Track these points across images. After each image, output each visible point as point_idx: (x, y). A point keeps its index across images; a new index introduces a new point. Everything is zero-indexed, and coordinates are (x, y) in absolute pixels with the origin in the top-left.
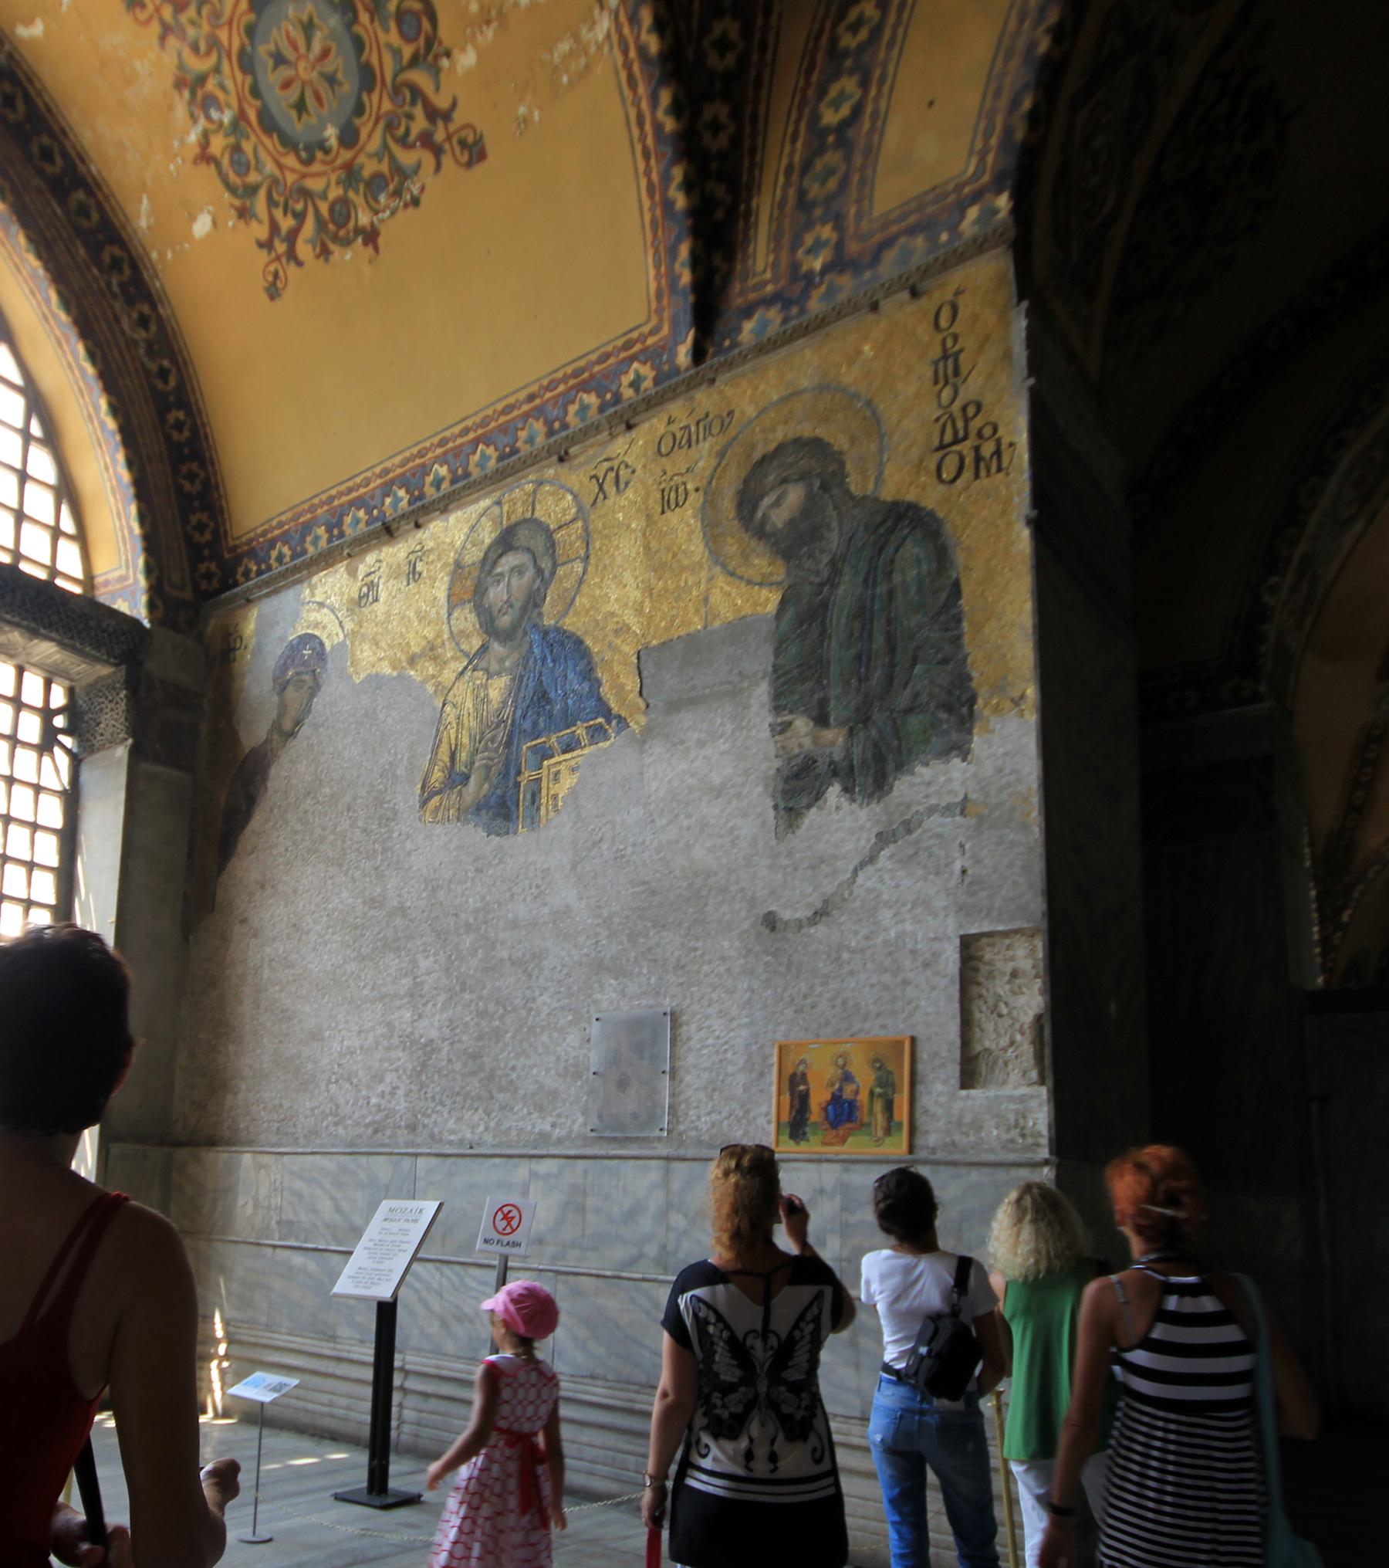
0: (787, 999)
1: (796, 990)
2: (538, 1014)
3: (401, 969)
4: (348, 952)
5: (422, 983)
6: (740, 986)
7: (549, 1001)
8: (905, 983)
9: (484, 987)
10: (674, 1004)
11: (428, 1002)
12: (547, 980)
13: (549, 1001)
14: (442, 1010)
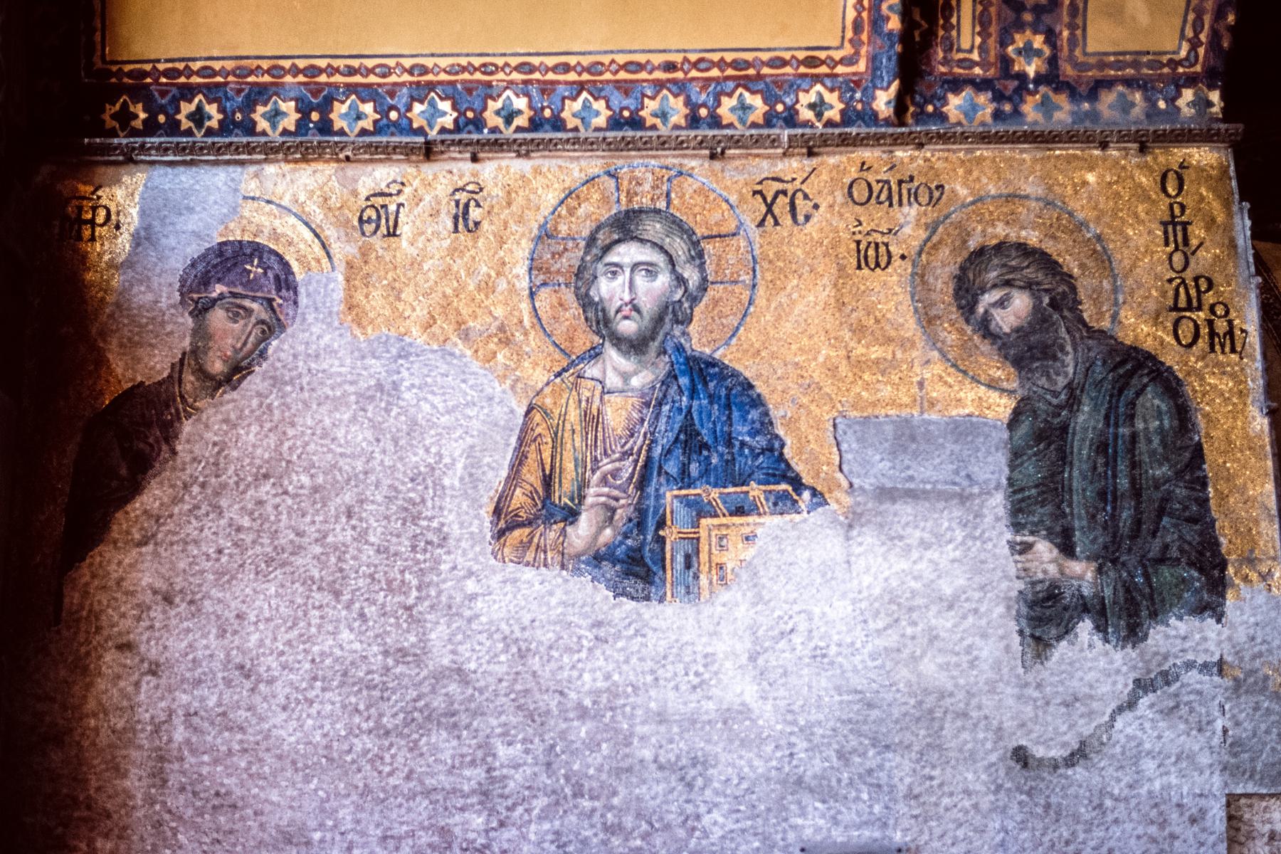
0: (1047, 845)
1: (1056, 834)
2: (706, 834)
3: (462, 756)
4: (357, 720)
5: (505, 777)
6: (991, 825)
7: (721, 820)
9: (615, 793)
10: (908, 839)
11: (515, 805)
12: (717, 793)
13: (721, 820)
14: (539, 818)
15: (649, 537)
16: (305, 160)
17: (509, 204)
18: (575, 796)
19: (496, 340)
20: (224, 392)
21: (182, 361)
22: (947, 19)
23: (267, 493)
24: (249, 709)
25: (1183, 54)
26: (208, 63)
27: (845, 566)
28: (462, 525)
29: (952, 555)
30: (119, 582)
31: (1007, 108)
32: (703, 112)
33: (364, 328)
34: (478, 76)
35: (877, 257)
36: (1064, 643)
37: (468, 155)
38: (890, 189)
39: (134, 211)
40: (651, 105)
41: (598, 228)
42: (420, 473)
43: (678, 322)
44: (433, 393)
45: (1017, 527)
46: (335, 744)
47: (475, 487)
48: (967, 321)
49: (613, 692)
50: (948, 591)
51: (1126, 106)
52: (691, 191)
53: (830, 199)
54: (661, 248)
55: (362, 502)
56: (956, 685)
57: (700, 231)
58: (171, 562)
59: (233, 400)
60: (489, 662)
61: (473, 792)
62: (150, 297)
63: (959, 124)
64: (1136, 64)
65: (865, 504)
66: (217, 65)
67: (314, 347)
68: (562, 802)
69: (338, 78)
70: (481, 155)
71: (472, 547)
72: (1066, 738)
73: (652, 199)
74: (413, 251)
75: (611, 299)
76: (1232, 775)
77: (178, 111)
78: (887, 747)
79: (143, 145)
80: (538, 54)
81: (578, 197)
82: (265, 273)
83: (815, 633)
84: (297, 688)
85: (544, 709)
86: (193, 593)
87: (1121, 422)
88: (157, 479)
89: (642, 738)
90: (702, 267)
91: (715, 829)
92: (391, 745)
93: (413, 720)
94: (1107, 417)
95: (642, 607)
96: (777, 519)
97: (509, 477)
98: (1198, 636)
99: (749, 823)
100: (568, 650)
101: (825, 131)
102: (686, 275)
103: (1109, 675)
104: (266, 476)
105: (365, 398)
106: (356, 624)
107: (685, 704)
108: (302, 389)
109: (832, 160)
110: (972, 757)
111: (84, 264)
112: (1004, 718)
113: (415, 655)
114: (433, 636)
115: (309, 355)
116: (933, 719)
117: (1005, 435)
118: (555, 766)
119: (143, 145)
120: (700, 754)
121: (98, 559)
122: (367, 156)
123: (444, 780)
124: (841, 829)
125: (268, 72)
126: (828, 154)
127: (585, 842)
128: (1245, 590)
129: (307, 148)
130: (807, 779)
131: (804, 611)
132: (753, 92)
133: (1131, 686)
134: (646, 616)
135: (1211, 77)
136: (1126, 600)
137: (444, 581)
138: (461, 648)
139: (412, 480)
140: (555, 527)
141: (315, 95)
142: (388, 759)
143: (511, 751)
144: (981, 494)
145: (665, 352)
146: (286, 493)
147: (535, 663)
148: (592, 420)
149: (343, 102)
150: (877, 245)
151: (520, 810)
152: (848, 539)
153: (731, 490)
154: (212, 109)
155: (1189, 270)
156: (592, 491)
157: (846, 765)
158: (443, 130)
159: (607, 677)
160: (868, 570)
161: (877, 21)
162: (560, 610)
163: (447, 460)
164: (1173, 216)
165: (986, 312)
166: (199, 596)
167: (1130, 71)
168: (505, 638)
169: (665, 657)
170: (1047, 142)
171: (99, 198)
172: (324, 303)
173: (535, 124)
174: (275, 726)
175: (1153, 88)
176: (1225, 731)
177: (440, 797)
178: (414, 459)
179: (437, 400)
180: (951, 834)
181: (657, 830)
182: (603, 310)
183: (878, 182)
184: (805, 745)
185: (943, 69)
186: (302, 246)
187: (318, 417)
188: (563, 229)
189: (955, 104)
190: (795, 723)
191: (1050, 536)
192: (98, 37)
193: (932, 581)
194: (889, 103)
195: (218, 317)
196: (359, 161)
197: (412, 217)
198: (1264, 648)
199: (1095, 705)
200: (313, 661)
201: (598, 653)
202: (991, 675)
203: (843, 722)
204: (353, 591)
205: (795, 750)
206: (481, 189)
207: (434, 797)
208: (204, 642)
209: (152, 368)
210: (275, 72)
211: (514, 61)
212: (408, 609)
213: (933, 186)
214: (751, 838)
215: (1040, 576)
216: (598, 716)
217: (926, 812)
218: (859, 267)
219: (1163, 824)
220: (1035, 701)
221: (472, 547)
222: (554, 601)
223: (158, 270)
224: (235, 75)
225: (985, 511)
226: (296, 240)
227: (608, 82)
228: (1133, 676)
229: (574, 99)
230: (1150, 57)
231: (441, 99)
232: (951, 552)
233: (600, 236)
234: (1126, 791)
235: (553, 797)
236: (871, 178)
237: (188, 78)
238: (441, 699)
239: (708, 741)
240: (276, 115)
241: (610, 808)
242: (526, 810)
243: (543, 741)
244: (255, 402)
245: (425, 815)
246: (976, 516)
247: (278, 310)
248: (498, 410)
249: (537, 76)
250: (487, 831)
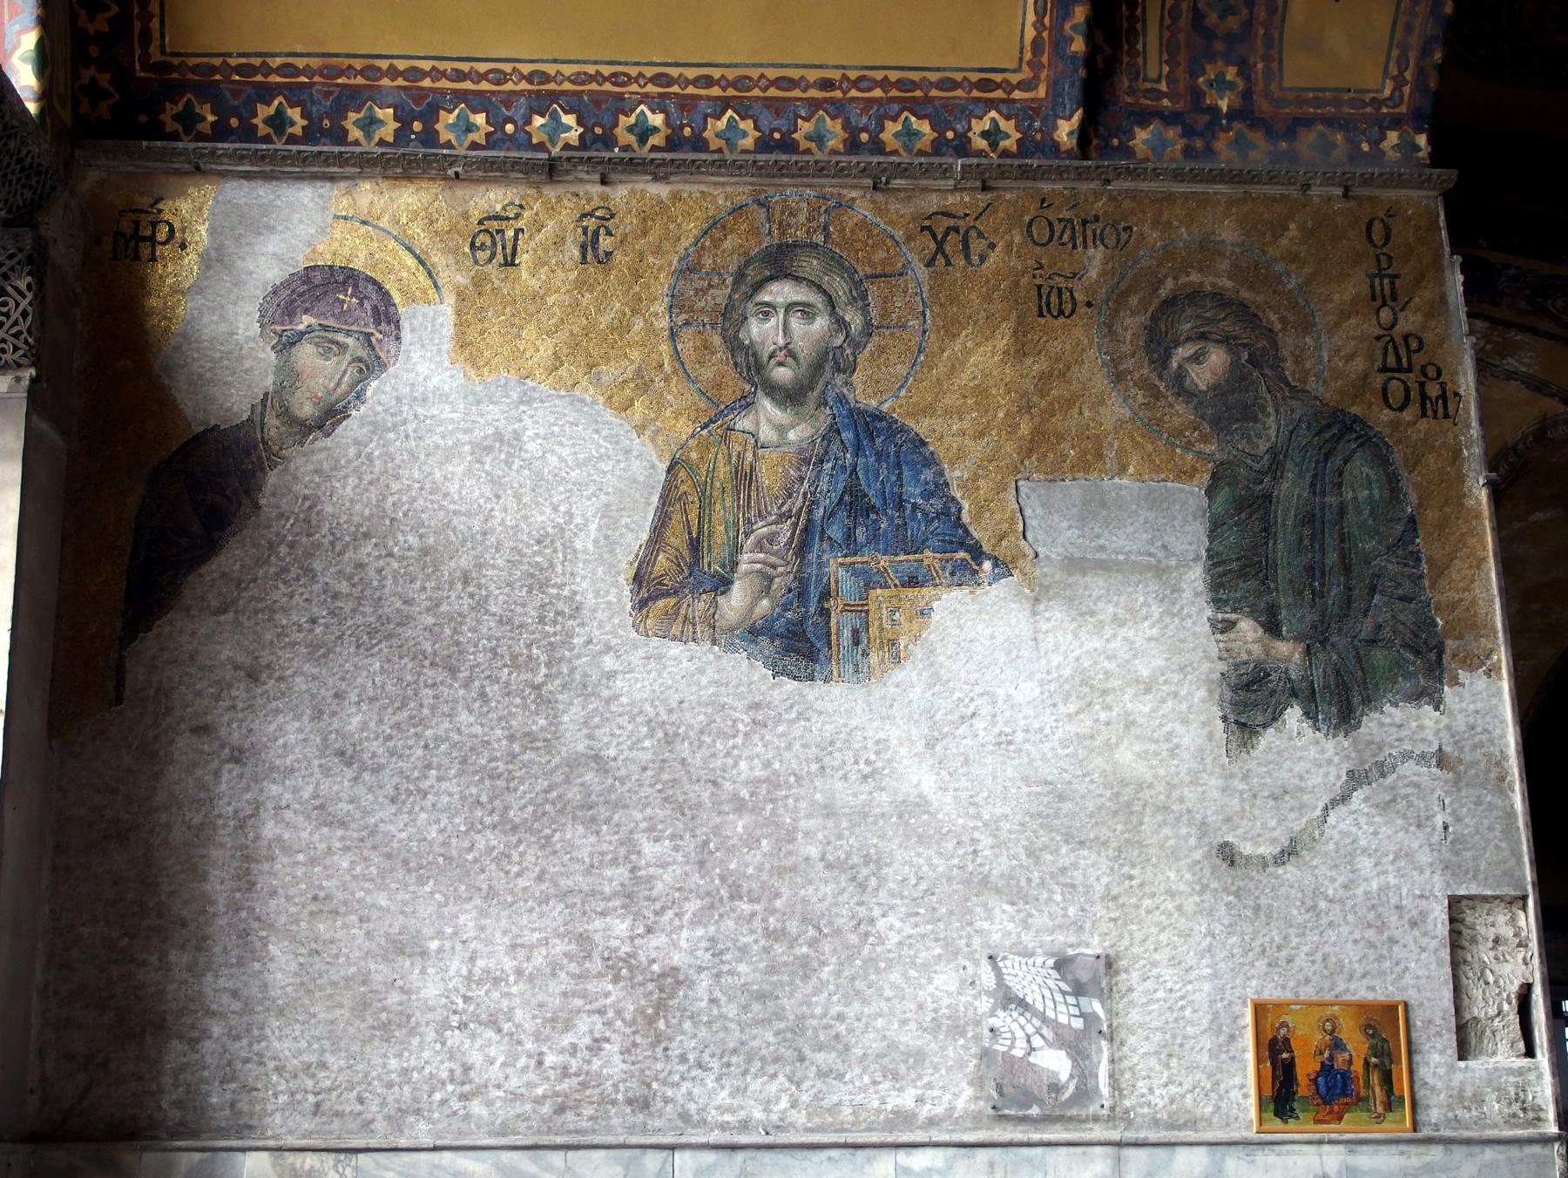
0: (1258, 949)
3: (602, 854)
4: (479, 813)
5: (652, 877)
8: (1393, 941)
9: (777, 895)
11: (663, 909)
12: (893, 895)
13: (898, 924)
14: (692, 923)
15: (812, 610)
16: (409, 178)
17: (645, 233)
18: (732, 898)
19: (632, 385)
20: (315, 439)
21: (264, 402)
22: (1132, 45)
23: (369, 555)
24: (351, 802)
25: (1387, 93)
26: (290, 60)
27: (1032, 643)
28: (597, 594)
29: (1149, 633)
30: (192, 657)
31: (1199, 144)
32: (864, 137)
33: (478, 368)
34: (608, 87)
36: (1271, 731)
37: (597, 177)
38: (1073, 229)
39: (203, 229)
40: (805, 127)
41: (747, 264)
42: (547, 534)
43: (839, 370)
44: (561, 444)
45: (1218, 603)
46: (454, 840)
47: (612, 551)
48: (1160, 378)
49: (773, 782)
50: (1145, 673)
51: (1328, 147)
52: (851, 224)
54: (819, 287)
55: (479, 566)
56: (1156, 776)
57: (863, 270)
58: (255, 633)
59: (326, 449)
60: (631, 749)
61: (616, 894)
62: (223, 328)
63: (1147, 160)
64: (1336, 102)
65: (1053, 576)
66: (300, 63)
67: (421, 389)
68: (717, 905)
69: (444, 84)
70: (613, 177)
71: (610, 618)
72: (1276, 834)
73: (808, 232)
74: (534, 283)
75: (763, 343)
76: (1453, 874)
77: (256, 115)
78: (1082, 843)
79: (213, 152)
80: (677, 65)
81: (724, 227)
82: (361, 304)
83: (999, 718)
84: (407, 778)
85: (695, 801)
86: (283, 669)
88: (238, 538)
89: (806, 834)
90: (865, 309)
91: (891, 934)
92: (520, 842)
93: (544, 814)
94: (1313, 485)
95: (805, 686)
96: (957, 593)
97: (650, 540)
98: (1414, 724)
99: (929, 927)
100: (722, 734)
101: (1002, 161)
102: (847, 318)
103: (1320, 766)
104: (367, 536)
105: (482, 449)
106: (477, 705)
107: (855, 795)
108: (407, 437)
109: (1008, 196)
110: (1174, 855)
111: (144, 288)
112: (1209, 813)
113: (545, 740)
114: (566, 719)
115: (415, 399)
116: (1132, 813)
117: (1205, 502)
118: (708, 865)
119: (213, 152)
120: (872, 851)
121: (167, 629)
122: (480, 173)
123: (583, 882)
124: (1032, 934)
125: (361, 72)
126: (1004, 189)
127: (744, 950)
128: (1463, 675)
129: (410, 162)
130: (993, 879)
131: (987, 693)
132: (919, 117)
133: (1344, 778)
134: (810, 698)
135: (1418, 119)
136: (1337, 686)
137: (578, 657)
138: (597, 732)
139: (539, 542)
140: (704, 596)
141: (417, 101)
142: (516, 857)
143: (658, 848)
144: (1177, 567)
145: (826, 404)
146: (390, 555)
147: (684, 749)
148: (744, 478)
149: (451, 111)
150: (1060, 290)
151: (670, 914)
152: (1034, 613)
153: (902, 557)
154: (294, 114)
156: (745, 557)
157: (1036, 864)
158: (567, 147)
159: (767, 765)
160: (1057, 647)
161: (1060, 41)
162: (711, 690)
163: (578, 520)
165: (1180, 367)
166: (289, 672)
167: (1330, 109)
168: (649, 721)
169: (832, 743)
171: (160, 211)
172: (432, 340)
173: (673, 143)
174: (382, 821)
175: (1356, 128)
176: (1446, 828)
177: (577, 900)
178: (540, 519)
179: (565, 452)
180: (1152, 939)
181: (826, 936)
182: (755, 355)
183: (1060, 220)
184: (990, 841)
185: (1129, 100)
186: (405, 274)
187: (427, 469)
188: (708, 262)
189: (1142, 136)
190: (978, 817)
191: (1253, 614)
192: (155, 23)
193: (1128, 662)
194: (1070, 134)
195: (306, 354)
196: (471, 180)
197: (532, 244)
198: (1485, 737)
199: (1305, 797)
200: (426, 746)
201: (756, 738)
202: (1194, 765)
203: (1032, 816)
204: (472, 668)
205: (980, 848)
206: (612, 216)
207: (570, 900)
208: (297, 725)
209: (229, 409)
210: (370, 74)
211: (649, 72)
212: (537, 687)
214: (932, 944)
215: (1245, 657)
216: (756, 810)
217: (1126, 915)
218: (1041, 315)
219: (1381, 929)
220: (1241, 793)
221: (610, 618)
222: (704, 680)
223: (233, 297)
224: (322, 76)
225: (1184, 585)
226: (397, 266)
227: (757, 98)
228: (1345, 766)
229: (718, 118)
230: (1351, 95)
231: (566, 112)
232: (1148, 629)
233: (749, 271)
234: (1341, 892)
235: (707, 900)
237: (266, 76)
238: (576, 789)
239: (882, 837)
240: (370, 124)
241: (773, 911)
242: (677, 915)
243: (694, 837)
244: (352, 451)
245: (560, 920)
246: (1173, 591)
247: (377, 347)
248: (636, 464)
249: (675, 89)
250: (632, 938)
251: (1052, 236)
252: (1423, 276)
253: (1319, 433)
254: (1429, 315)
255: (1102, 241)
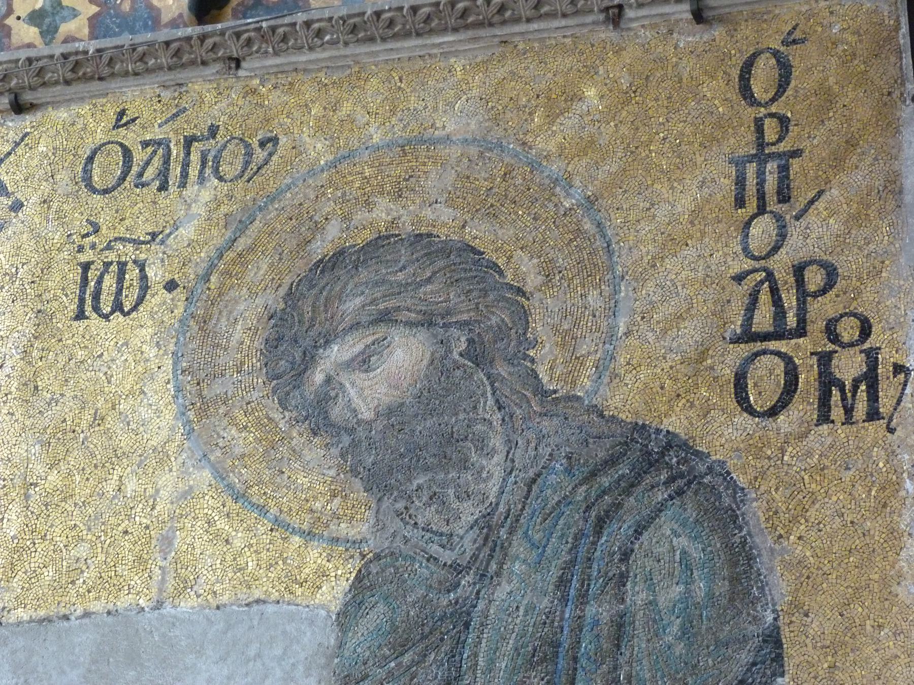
35: (119, 291)
53: (46, 187)
87: (594, 589)
94: (563, 583)
109: (63, 114)
126: (56, 104)
155: (783, 251)
164: (761, 144)
165: (328, 380)
170: (491, 25)
183: (146, 144)
213: (255, 143)
218: (80, 315)
236: (130, 137)
251: (123, 179)
252: (851, 143)
253: (593, 474)
254: (856, 219)
255: (216, 171)
